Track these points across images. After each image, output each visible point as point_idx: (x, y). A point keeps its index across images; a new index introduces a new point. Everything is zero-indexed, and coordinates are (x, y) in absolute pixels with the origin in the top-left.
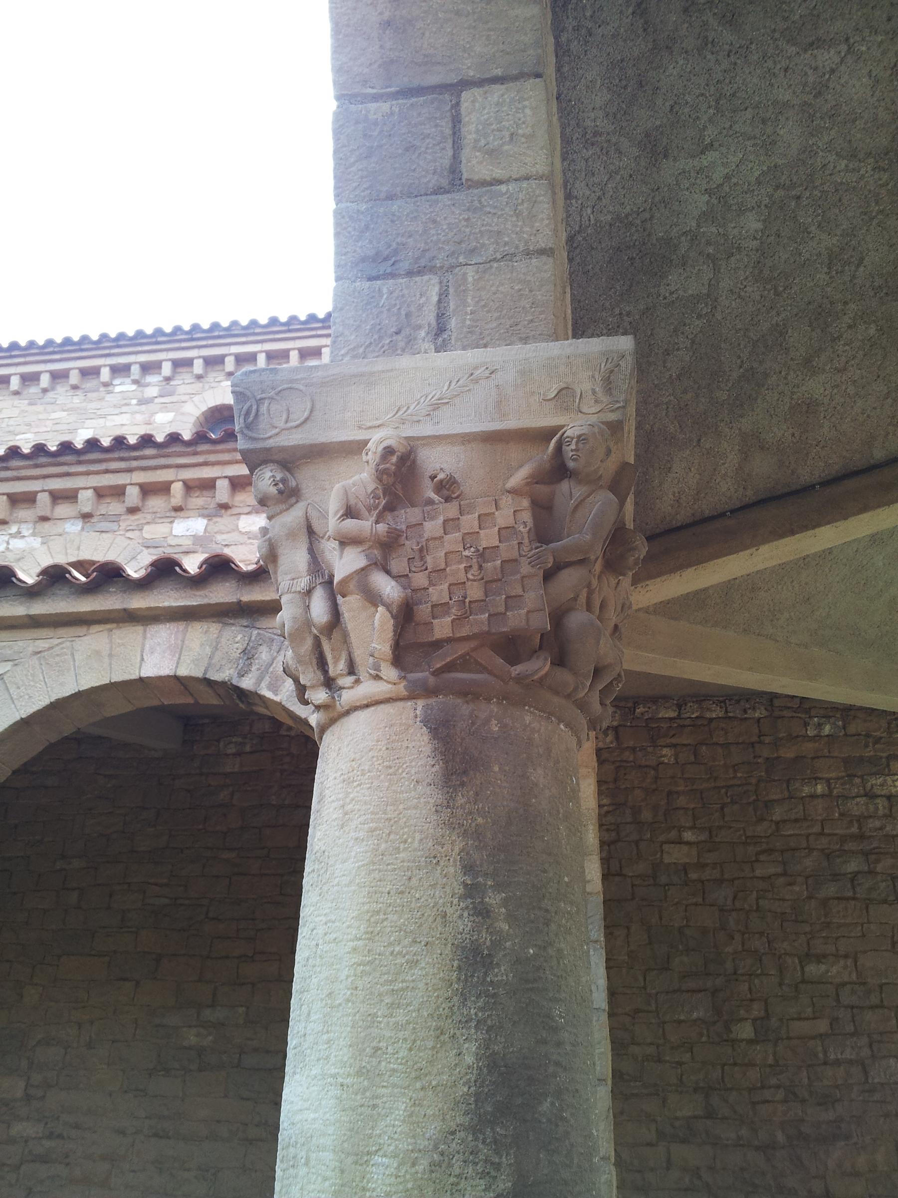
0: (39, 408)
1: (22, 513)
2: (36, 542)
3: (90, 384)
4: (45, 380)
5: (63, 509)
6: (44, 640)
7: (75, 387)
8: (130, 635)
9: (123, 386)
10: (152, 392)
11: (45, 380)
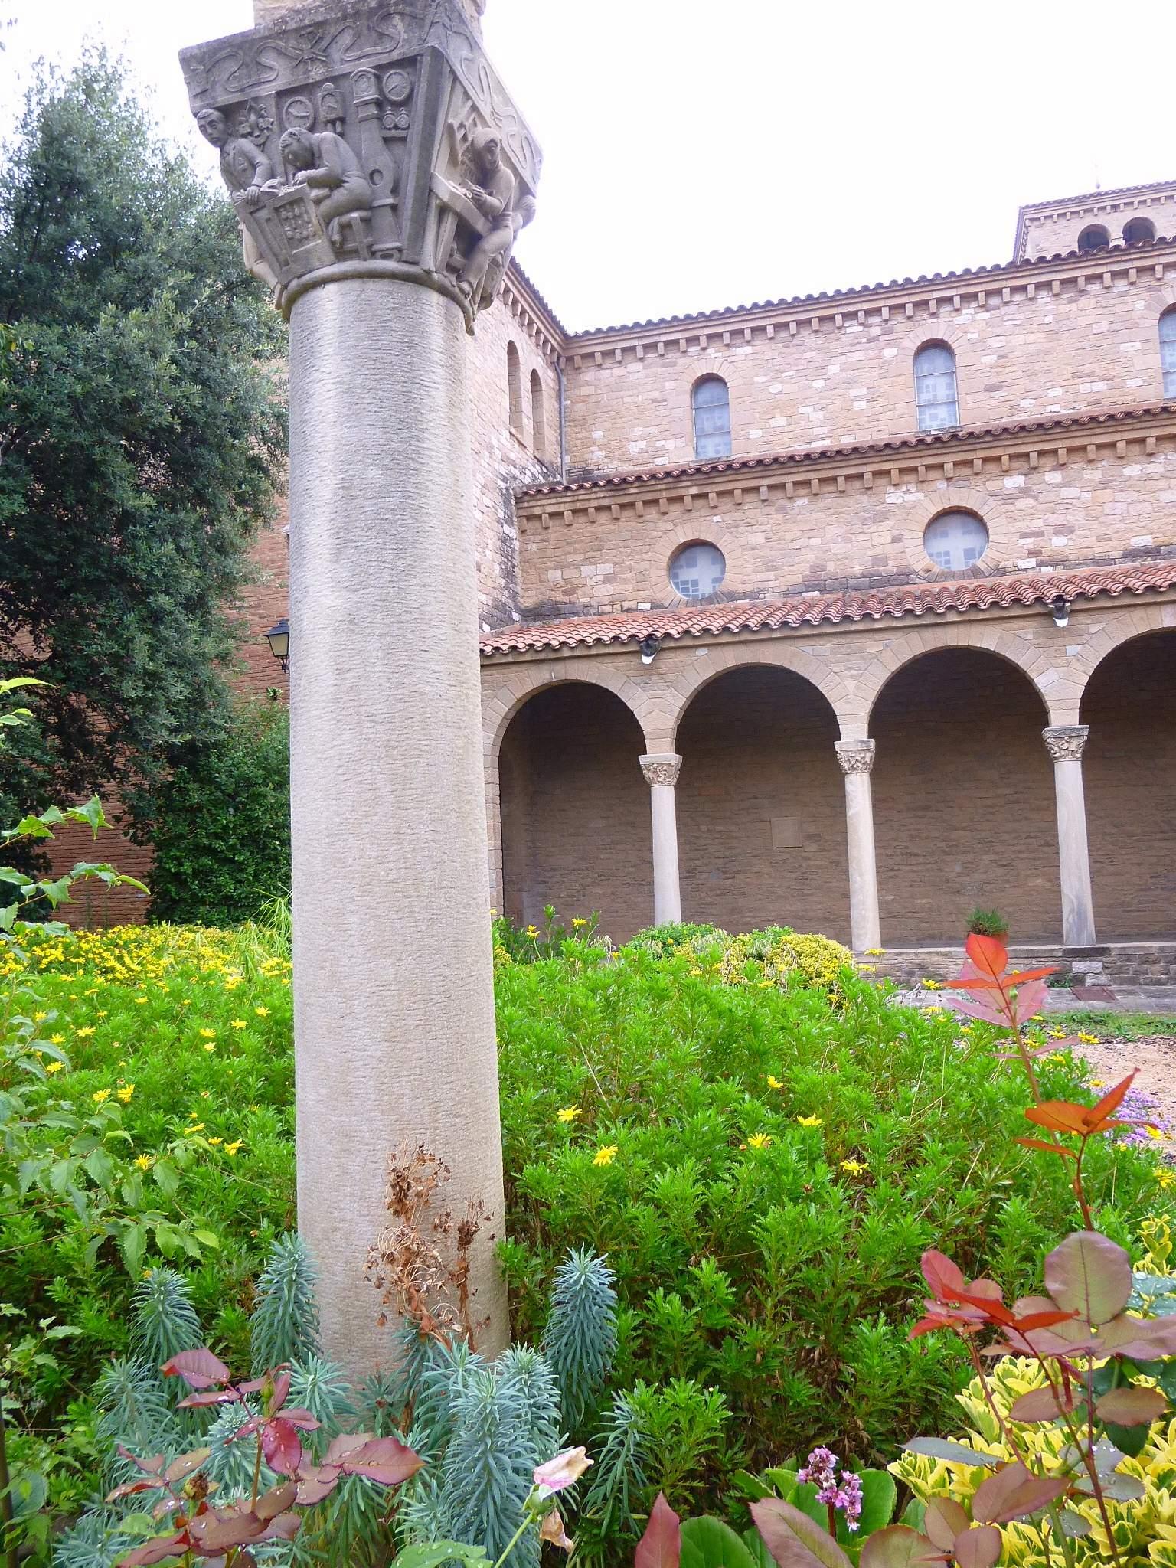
0: (792, 349)
1: (906, 478)
2: (921, 496)
3: (827, 327)
4: (793, 327)
5: (933, 474)
6: (1118, 614)
7: (816, 332)
8: (1153, 612)
9: (852, 327)
10: (876, 331)
11: (793, 327)
